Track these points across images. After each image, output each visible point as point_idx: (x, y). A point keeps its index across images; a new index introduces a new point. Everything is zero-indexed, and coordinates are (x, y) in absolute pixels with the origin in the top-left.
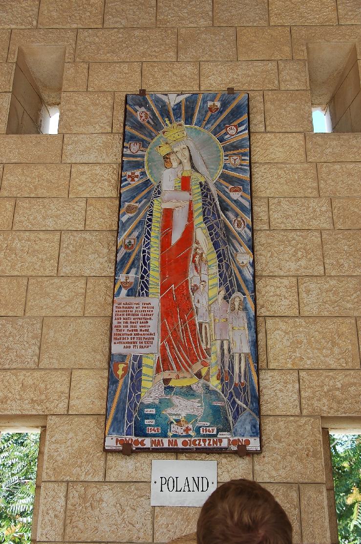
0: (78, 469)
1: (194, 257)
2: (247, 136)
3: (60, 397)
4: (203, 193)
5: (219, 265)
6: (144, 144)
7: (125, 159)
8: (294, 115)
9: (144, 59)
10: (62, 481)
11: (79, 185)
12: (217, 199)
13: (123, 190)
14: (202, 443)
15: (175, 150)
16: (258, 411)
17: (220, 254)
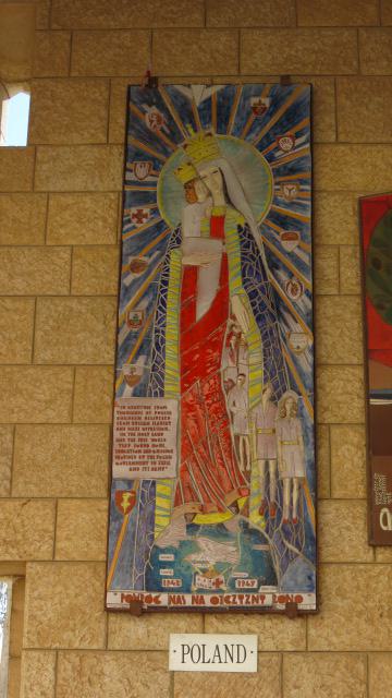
0: (71, 634)
1: (231, 334)
2: (308, 153)
3: (42, 537)
4: (242, 242)
5: (264, 351)
6: (156, 165)
7: (128, 189)
8: (380, 115)
9: (155, 25)
10: (49, 649)
11: (61, 226)
12: (262, 252)
13: (126, 237)
14: (237, 600)
15: (202, 174)
16: (316, 558)
17: (266, 334)
